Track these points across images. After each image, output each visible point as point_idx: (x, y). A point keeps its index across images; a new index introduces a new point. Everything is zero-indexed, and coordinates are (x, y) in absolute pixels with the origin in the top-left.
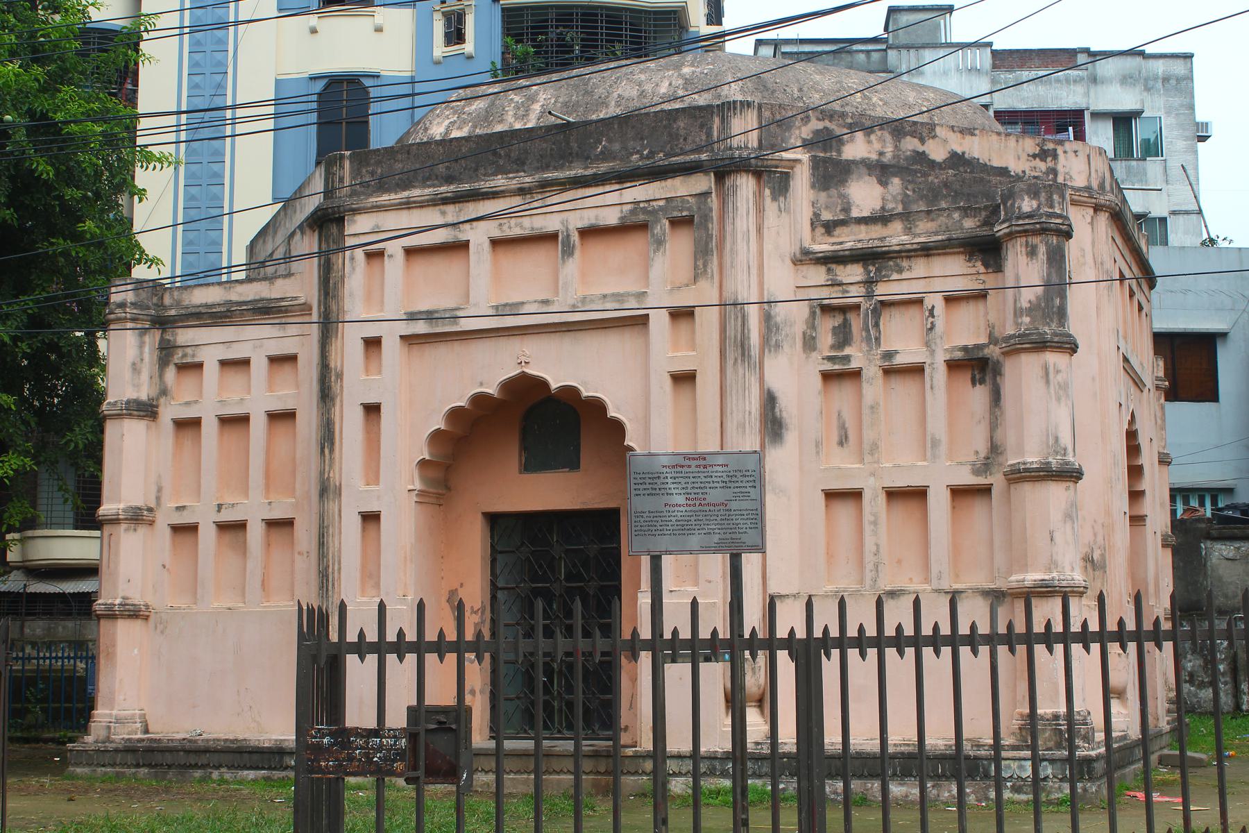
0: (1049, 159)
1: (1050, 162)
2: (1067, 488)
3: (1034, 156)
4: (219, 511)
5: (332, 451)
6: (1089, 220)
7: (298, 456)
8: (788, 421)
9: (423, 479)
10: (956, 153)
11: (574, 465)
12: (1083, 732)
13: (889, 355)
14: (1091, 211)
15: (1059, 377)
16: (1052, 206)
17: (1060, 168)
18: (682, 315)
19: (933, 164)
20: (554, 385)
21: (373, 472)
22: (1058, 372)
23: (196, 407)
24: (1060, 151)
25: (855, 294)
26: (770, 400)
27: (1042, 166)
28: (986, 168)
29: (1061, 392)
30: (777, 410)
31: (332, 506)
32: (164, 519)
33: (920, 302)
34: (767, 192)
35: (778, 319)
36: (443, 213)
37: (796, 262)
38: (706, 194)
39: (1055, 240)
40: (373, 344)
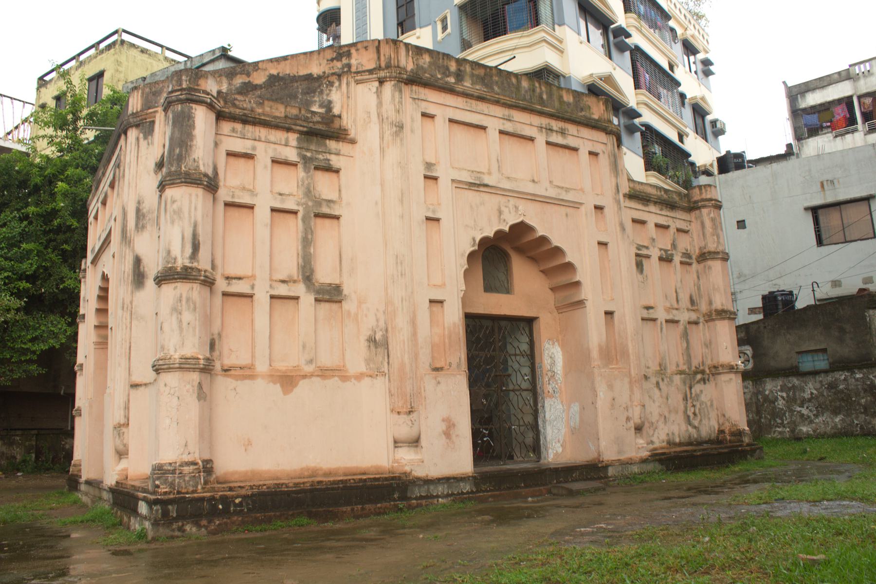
0: (344, 59)
1: (345, 61)
2: (175, 288)
3: (332, 60)
6: (374, 90)
8: (148, 273)
9: (99, 336)
10: (273, 75)
12: (170, 480)
14: (376, 84)
15: (175, 206)
16: (181, 85)
17: (353, 62)
19: (256, 87)
22: (174, 202)
24: (353, 51)
26: (138, 261)
27: (339, 65)
28: (294, 79)
29: (175, 217)
30: (141, 267)
34: (141, 135)
35: (145, 211)
37: (156, 172)
39: (179, 107)
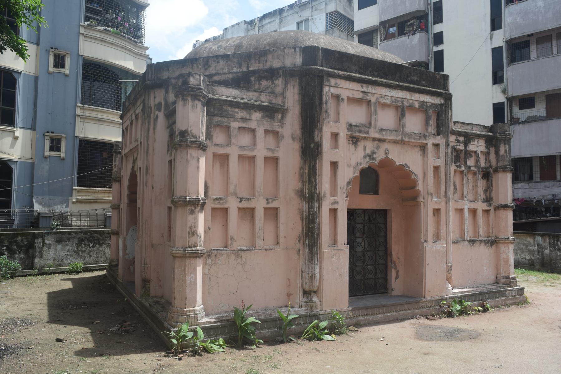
4: (241, 201)
5: (315, 180)
7: (281, 178)
11: (376, 192)
13: (469, 167)
18: (437, 146)
20: (398, 164)
21: (334, 193)
23: (229, 148)
25: (461, 147)
31: (316, 205)
32: (209, 205)
33: (475, 152)
36: (362, 86)
38: (441, 105)
40: (335, 136)
